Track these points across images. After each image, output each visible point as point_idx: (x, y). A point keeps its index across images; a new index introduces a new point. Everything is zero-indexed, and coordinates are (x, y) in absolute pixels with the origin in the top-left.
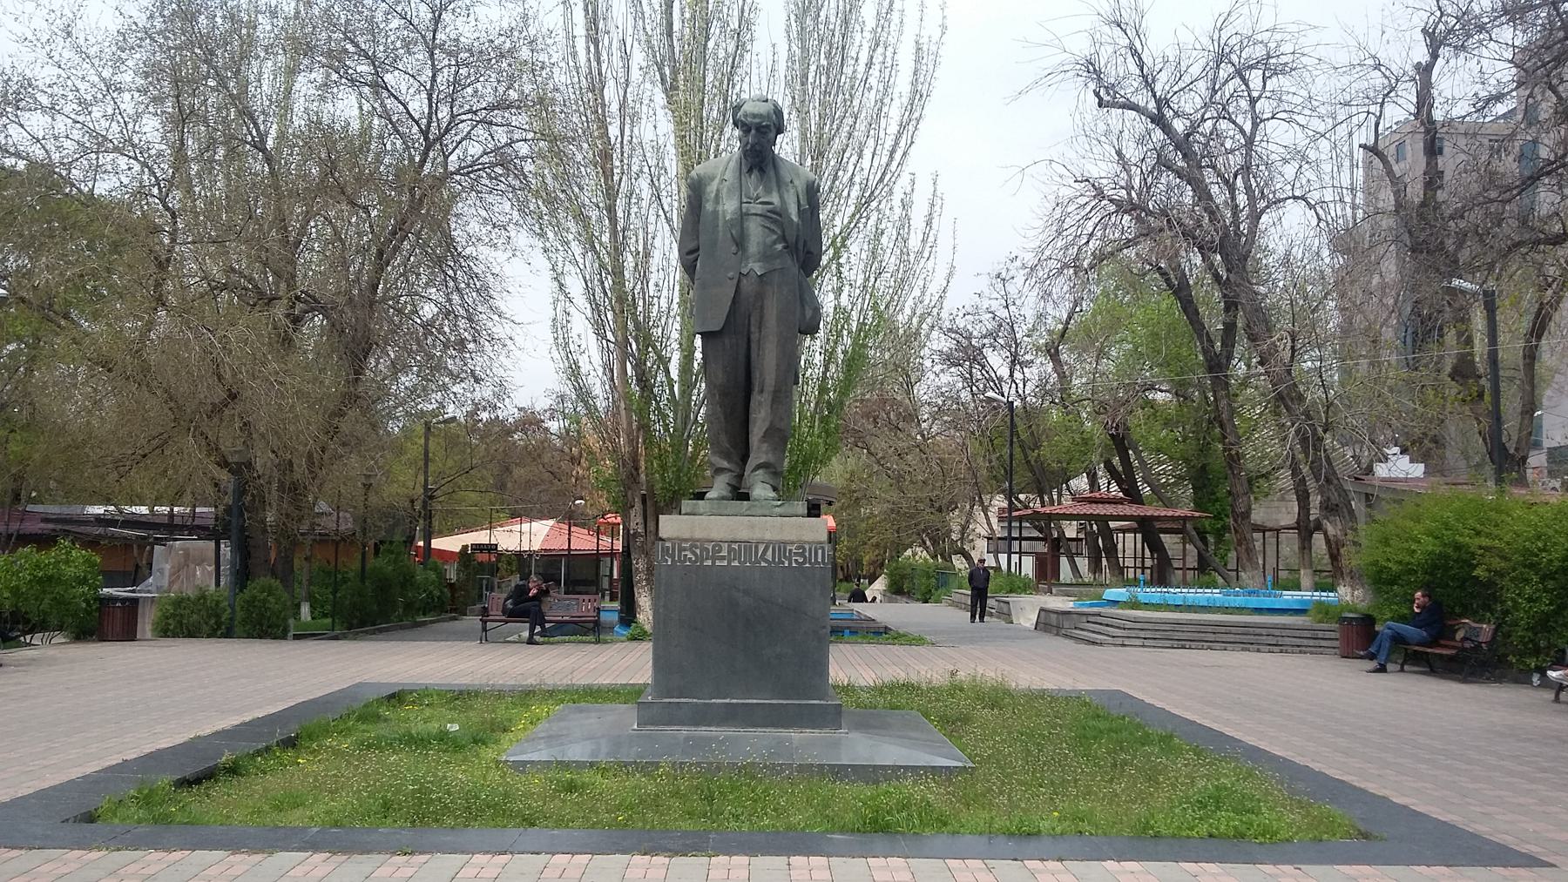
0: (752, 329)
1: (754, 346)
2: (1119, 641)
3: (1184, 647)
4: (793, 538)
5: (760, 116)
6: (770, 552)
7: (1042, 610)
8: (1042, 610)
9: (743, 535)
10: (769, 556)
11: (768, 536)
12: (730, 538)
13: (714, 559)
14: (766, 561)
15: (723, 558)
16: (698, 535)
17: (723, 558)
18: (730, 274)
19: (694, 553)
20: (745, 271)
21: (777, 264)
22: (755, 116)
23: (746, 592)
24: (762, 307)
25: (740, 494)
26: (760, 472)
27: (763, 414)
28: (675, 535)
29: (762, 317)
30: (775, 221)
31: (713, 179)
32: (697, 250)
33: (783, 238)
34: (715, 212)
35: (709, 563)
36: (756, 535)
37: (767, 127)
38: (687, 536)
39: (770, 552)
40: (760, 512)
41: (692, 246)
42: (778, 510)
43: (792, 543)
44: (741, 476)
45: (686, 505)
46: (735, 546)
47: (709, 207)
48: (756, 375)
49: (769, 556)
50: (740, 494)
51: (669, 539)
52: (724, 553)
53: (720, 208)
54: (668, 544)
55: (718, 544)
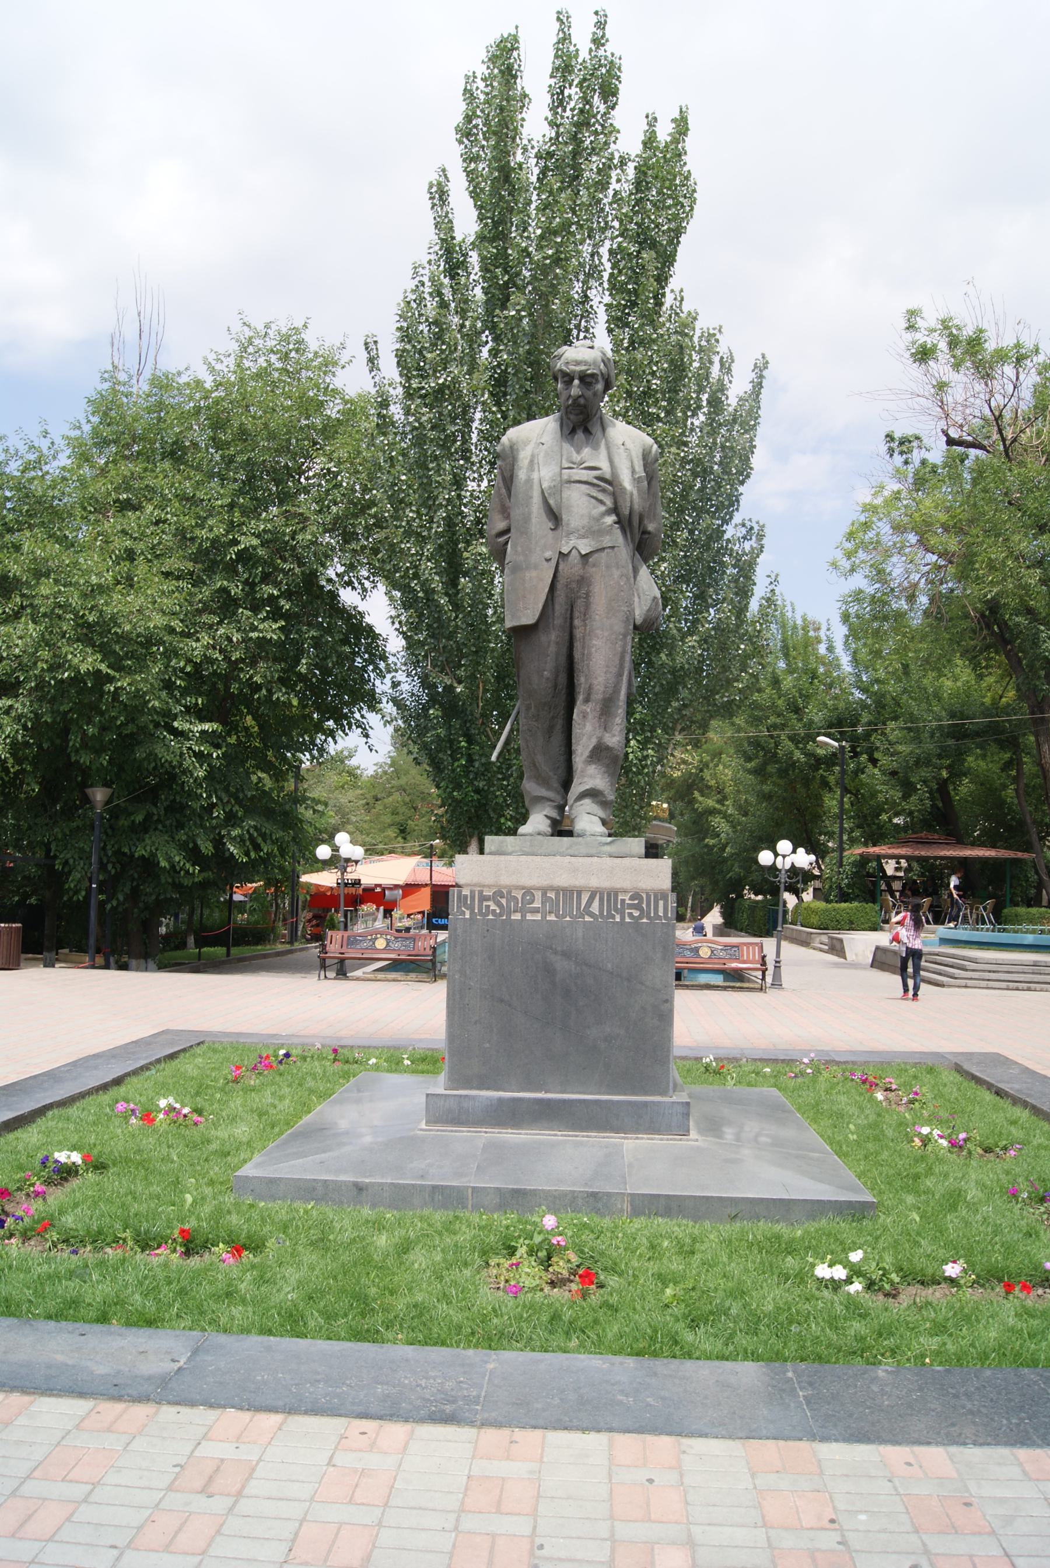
0: (576, 622)
1: (577, 645)
2: (963, 982)
3: (1029, 989)
4: (626, 884)
5: (586, 363)
6: (596, 903)
7: (877, 948)
8: (877, 948)
9: (563, 880)
10: (595, 908)
11: (594, 882)
12: (544, 882)
13: (523, 912)
14: (592, 915)
15: (536, 911)
16: (506, 880)
17: (536, 911)
18: (548, 554)
19: (499, 904)
20: (565, 550)
21: (607, 541)
22: (578, 363)
23: (566, 955)
24: (588, 595)
25: (561, 828)
26: (587, 801)
27: (589, 727)
28: (475, 880)
29: (587, 605)
30: (604, 491)
31: (526, 443)
32: (507, 531)
33: (615, 510)
34: (529, 481)
35: (517, 917)
36: (579, 881)
37: (593, 375)
39: (596, 903)
40: (584, 851)
42: (607, 848)
43: (625, 891)
44: (561, 808)
46: (552, 895)
47: (521, 475)
48: (581, 680)
49: (595, 908)
50: (561, 828)
51: (468, 885)
52: (537, 904)
53: (535, 476)
54: (466, 892)
55: (528, 891)
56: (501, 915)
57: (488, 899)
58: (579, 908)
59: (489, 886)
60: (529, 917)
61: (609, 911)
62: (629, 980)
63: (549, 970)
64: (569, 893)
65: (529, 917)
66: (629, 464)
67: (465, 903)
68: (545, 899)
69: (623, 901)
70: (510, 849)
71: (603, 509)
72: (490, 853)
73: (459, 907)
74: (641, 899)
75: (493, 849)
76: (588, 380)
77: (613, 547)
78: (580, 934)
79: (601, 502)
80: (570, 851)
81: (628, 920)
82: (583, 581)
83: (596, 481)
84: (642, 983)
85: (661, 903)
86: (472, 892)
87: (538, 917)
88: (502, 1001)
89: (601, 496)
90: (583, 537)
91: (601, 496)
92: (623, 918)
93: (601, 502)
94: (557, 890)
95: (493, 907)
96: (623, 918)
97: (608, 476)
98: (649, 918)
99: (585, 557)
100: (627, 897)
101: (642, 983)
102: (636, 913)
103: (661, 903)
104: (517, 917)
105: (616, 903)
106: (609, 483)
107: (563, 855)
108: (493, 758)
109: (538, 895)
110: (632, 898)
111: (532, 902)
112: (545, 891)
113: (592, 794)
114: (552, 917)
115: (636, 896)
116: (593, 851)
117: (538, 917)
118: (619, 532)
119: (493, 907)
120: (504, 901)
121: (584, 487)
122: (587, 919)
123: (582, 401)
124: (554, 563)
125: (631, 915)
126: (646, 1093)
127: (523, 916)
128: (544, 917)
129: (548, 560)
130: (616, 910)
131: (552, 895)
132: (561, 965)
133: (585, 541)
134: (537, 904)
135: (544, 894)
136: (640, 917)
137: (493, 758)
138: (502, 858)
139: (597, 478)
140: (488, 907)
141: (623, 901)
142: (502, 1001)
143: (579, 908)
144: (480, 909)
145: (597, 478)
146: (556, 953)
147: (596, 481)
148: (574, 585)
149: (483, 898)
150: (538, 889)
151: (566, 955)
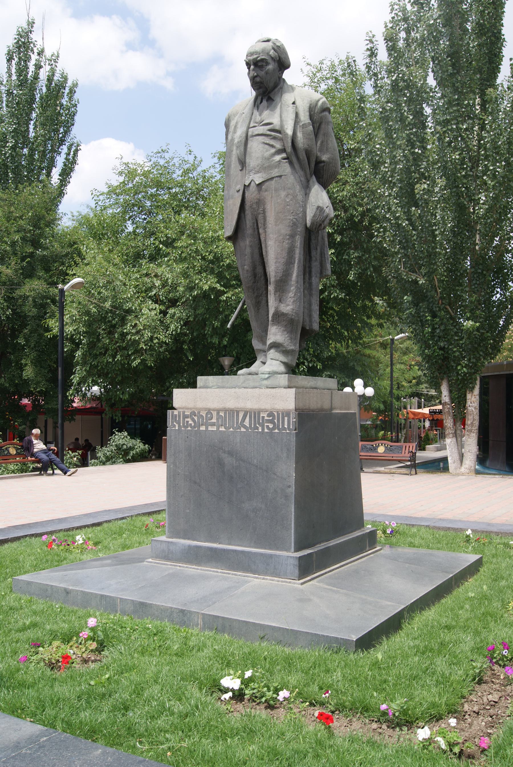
0: (261, 231)
1: (263, 246)
9: (231, 404)
10: (247, 423)
11: (250, 405)
13: (207, 425)
14: (245, 427)
15: (213, 424)
21: (275, 172)
23: (230, 453)
26: (272, 351)
30: (275, 138)
35: (203, 428)
38: (191, 405)
40: (252, 384)
45: (201, 380)
46: (222, 414)
49: (247, 423)
51: (180, 408)
52: (214, 420)
56: (194, 427)
57: (187, 417)
58: (237, 423)
59: (188, 409)
60: (210, 428)
61: (255, 424)
62: (267, 471)
63: (221, 463)
64: (232, 412)
65: (210, 428)
66: (293, 116)
67: (176, 420)
68: (219, 417)
69: (263, 417)
70: (211, 384)
71: (273, 150)
72: (200, 388)
73: (172, 422)
74: (274, 416)
75: (202, 384)
76: (260, 64)
77: (280, 176)
78: (238, 440)
79: (272, 146)
80: (244, 385)
81: (266, 430)
82: (260, 202)
83: (269, 133)
84: (275, 474)
85: (286, 418)
86: (179, 412)
87: (214, 428)
88: (195, 483)
89: (272, 142)
90: (258, 172)
91: (272, 142)
92: (263, 429)
93: (272, 146)
94: (225, 410)
95: (191, 422)
96: (263, 429)
97: (277, 128)
98: (279, 429)
99: (260, 185)
100: (265, 415)
101: (275, 474)
102: (271, 426)
103: (286, 418)
104: (203, 428)
105: (259, 419)
106: (279, 132)
107: (240, 388)
108: (229, 326)
109: (215, 414)
110: (269, 416)
111: (212, 418)
112: (218, 411)
113: (275, 346)
114: (222, 429)
115: (271, 414)
116: (257, 384)
117: (214, 428)
118: (287, 165)
119: (191, 422)
120: (196, 418)
121: (261, 138)
122: (243, 430)
123: (258, 79)
124: (241, 192)
125: (268, 426)
126: (277, 549)
128: (218, 428)
129: (238, 191)
130: (259, 424)
131: (222, 414)
132: (228, 460)
133: (259, 175)
134: (214, 420)
135: (218, 413)
137: (229, 326)
138: (209, 390)
139: (270, 130)
140: (188, 422)
141: (263, 417)
142: (195, 483)
143: (237, 423)
144: (184, 424)
145: (270, 130)
146: (224, 452)
147: (269, 133)
148: (255, 206)
149: (185, 417)
150: (214, 410)
151: (230, 453)
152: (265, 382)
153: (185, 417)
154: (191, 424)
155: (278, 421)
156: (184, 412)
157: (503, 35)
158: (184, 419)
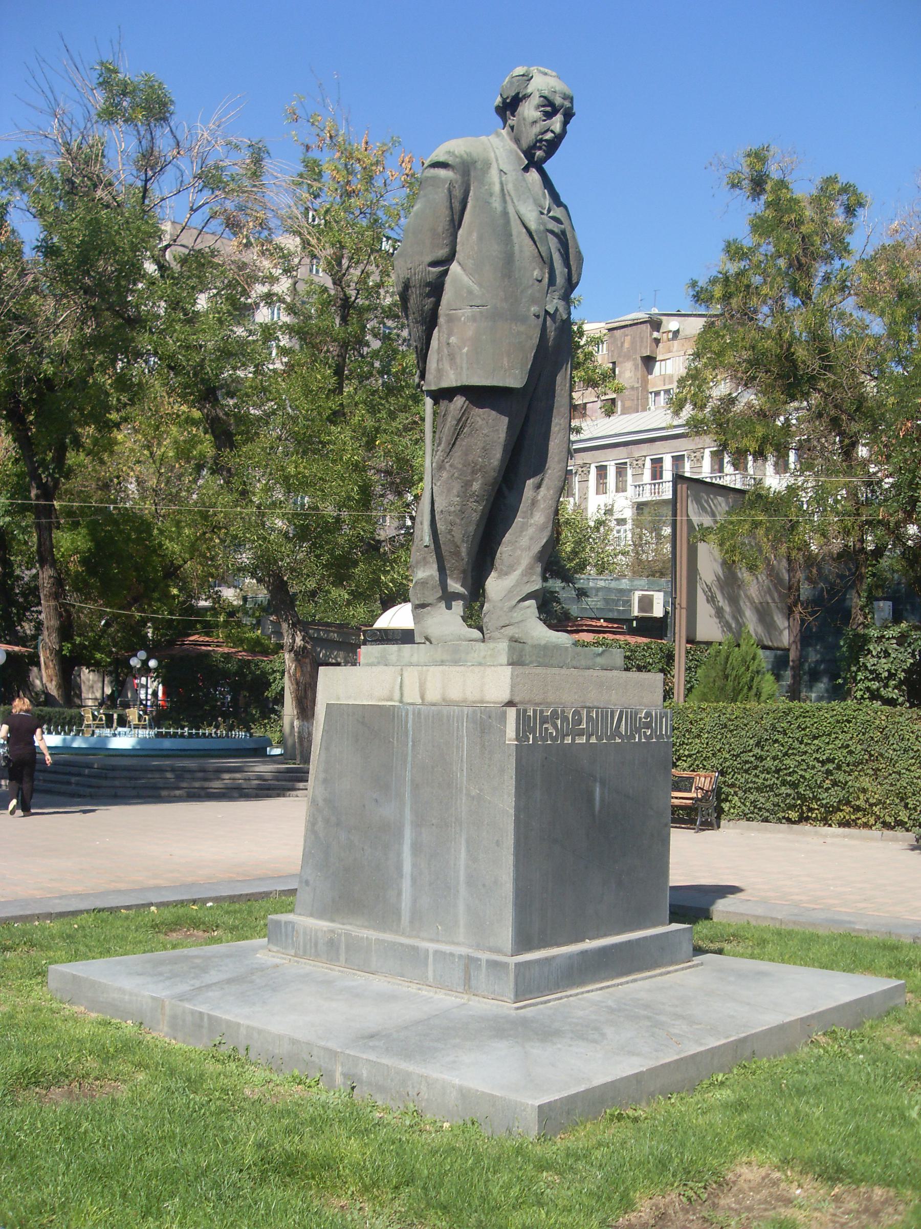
15: (581, 733)
35: (568, 740)
40: (583, 663)
41: (442, 253)
51: (522, 703)
80: (574, 663)
87: (583, 740)
104: (568, 740)
114: (593, 740)
116: (590, 663)
117: (583, 740)
124: (541, 319)
127: (573, 740)
136: (651, 736)
140: (547, 729)
144: (541, 733)
149: (544, 720)
152: (599, 660)
153: (544, 720)
154: (551, 733)
155: (656, 725)
156: (542, 712)
157: (734, 251)
158: (542, 724)
